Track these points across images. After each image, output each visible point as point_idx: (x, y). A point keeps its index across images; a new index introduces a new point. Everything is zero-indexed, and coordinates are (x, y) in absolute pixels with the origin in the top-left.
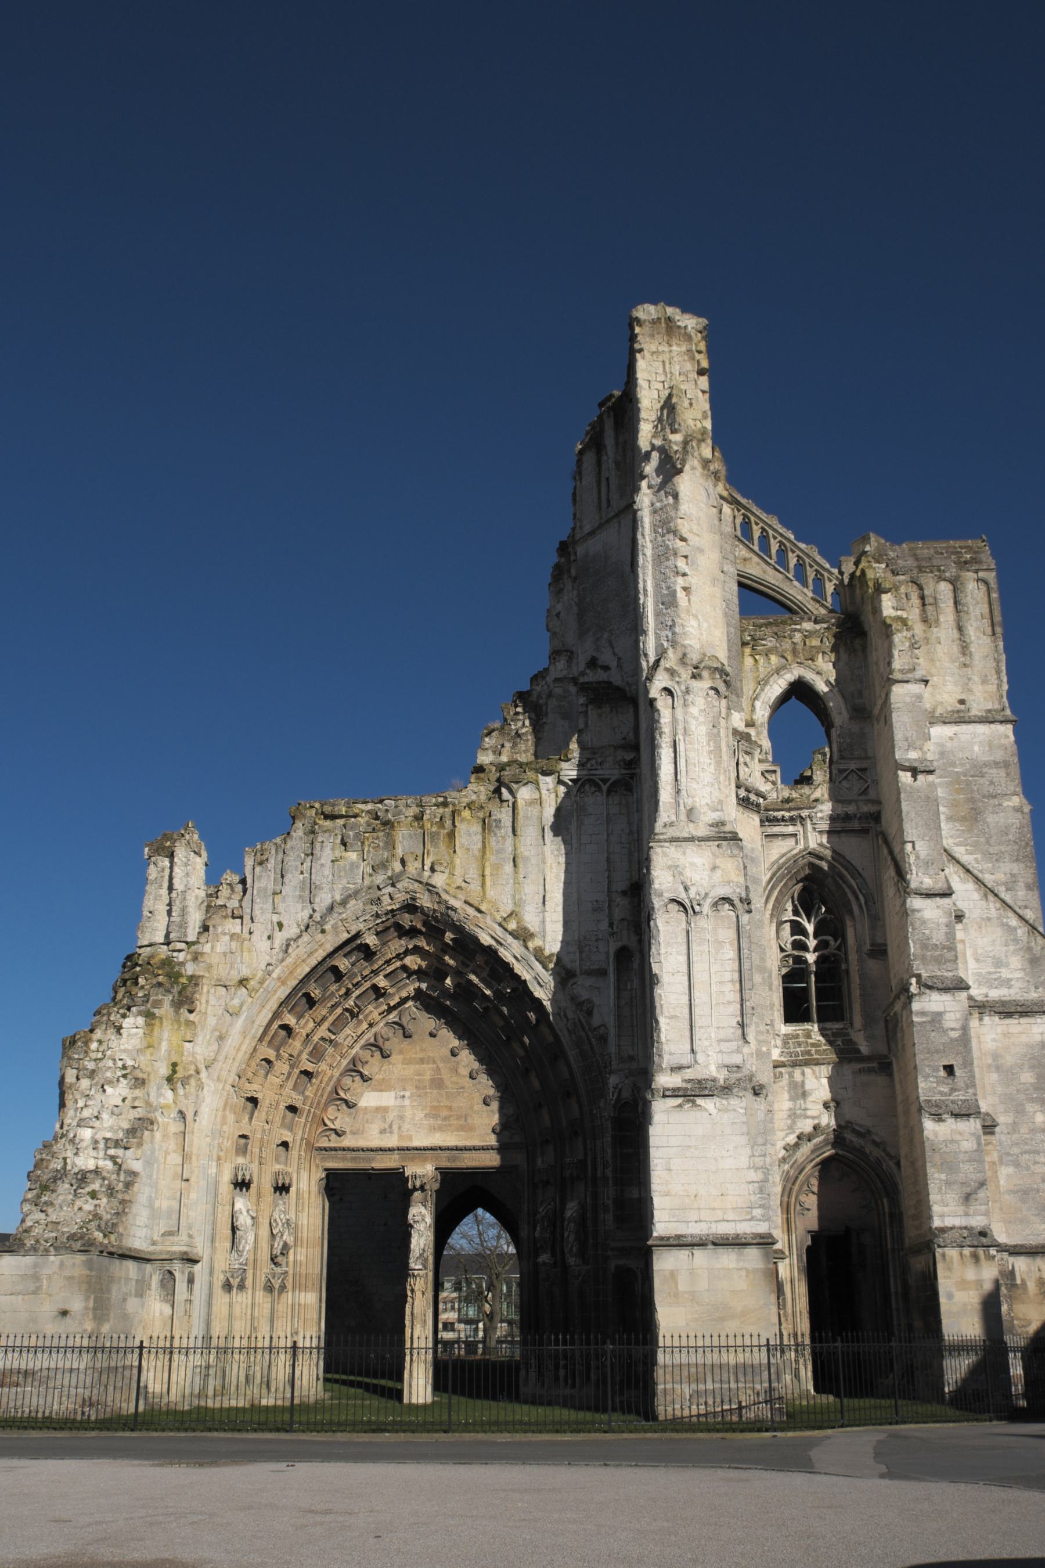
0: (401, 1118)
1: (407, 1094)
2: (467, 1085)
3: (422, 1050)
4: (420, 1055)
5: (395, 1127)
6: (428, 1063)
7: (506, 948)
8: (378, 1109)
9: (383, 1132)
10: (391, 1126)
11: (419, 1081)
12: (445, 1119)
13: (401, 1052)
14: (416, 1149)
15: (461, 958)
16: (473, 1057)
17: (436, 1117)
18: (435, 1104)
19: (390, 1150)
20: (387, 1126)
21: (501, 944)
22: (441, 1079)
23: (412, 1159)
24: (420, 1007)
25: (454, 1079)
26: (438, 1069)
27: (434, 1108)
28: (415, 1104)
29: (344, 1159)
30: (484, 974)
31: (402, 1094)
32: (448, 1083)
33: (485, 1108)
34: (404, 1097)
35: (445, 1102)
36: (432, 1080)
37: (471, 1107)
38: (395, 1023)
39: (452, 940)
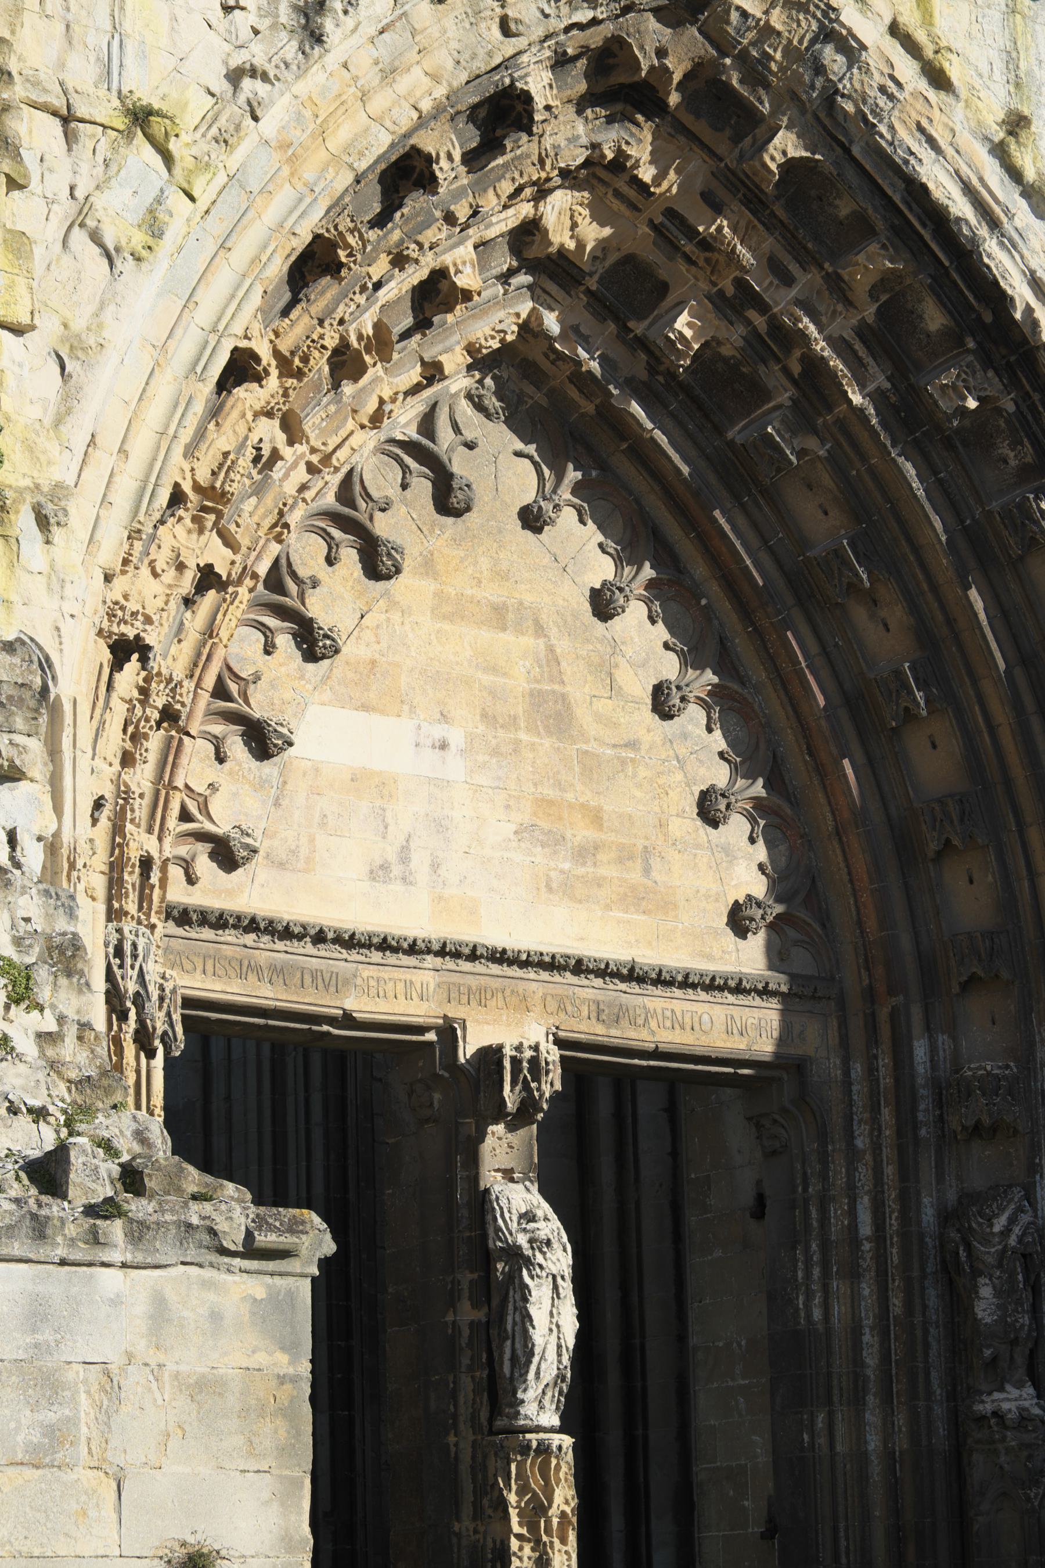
0: (440, 826)
1: (456, 737)
2: (646, 739)
3: (502, 576)
4: (492, 593)
5: (419, 861)
6: (520, 631)
7: (1010, 246)
8: (358, 779)
9: (379, 872)
10: (404, 855)
11: (492, 693)
12: (584, 853)
13: (428, 566)
14: (500, 957)
15: (769, 243)
16: (661, 632)
17: (554, 841)
18: (549, 792)
19: (413, 949)
20: (392, 856)
21: (994, 224)
22: (564, 697)
23: (481, 997)
24: (493, 402)
25: (604, 706)
26: (552, 657)
27: (544, 804)
28: (482, 779)
29: (245, 969)
30: (845, 325)
31: (438, 731)
32: (583, 715)
33: (705, 832)
34: (443, 746)
35: (580, 793)
36: (537, 698)
37: (662, 825)
38: (409, 446)
39: (790, 166)
